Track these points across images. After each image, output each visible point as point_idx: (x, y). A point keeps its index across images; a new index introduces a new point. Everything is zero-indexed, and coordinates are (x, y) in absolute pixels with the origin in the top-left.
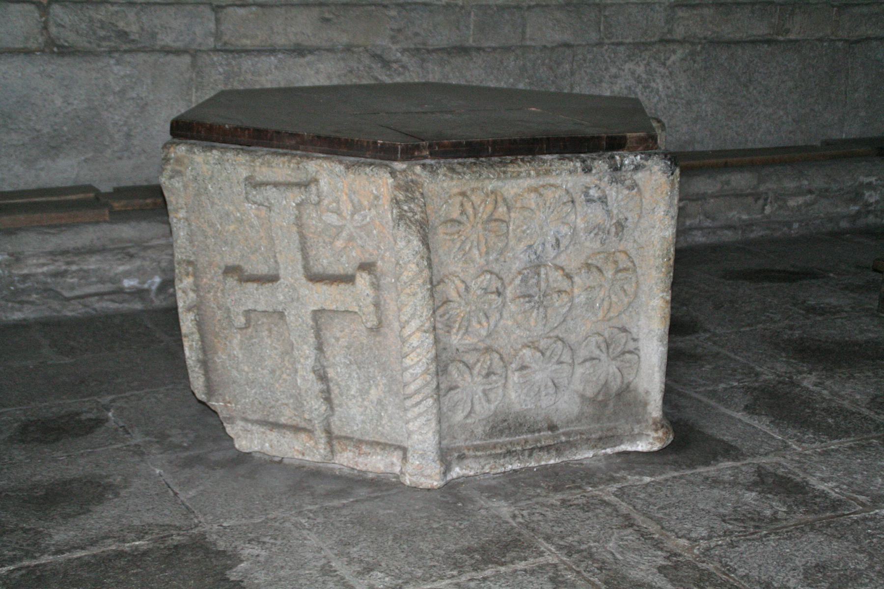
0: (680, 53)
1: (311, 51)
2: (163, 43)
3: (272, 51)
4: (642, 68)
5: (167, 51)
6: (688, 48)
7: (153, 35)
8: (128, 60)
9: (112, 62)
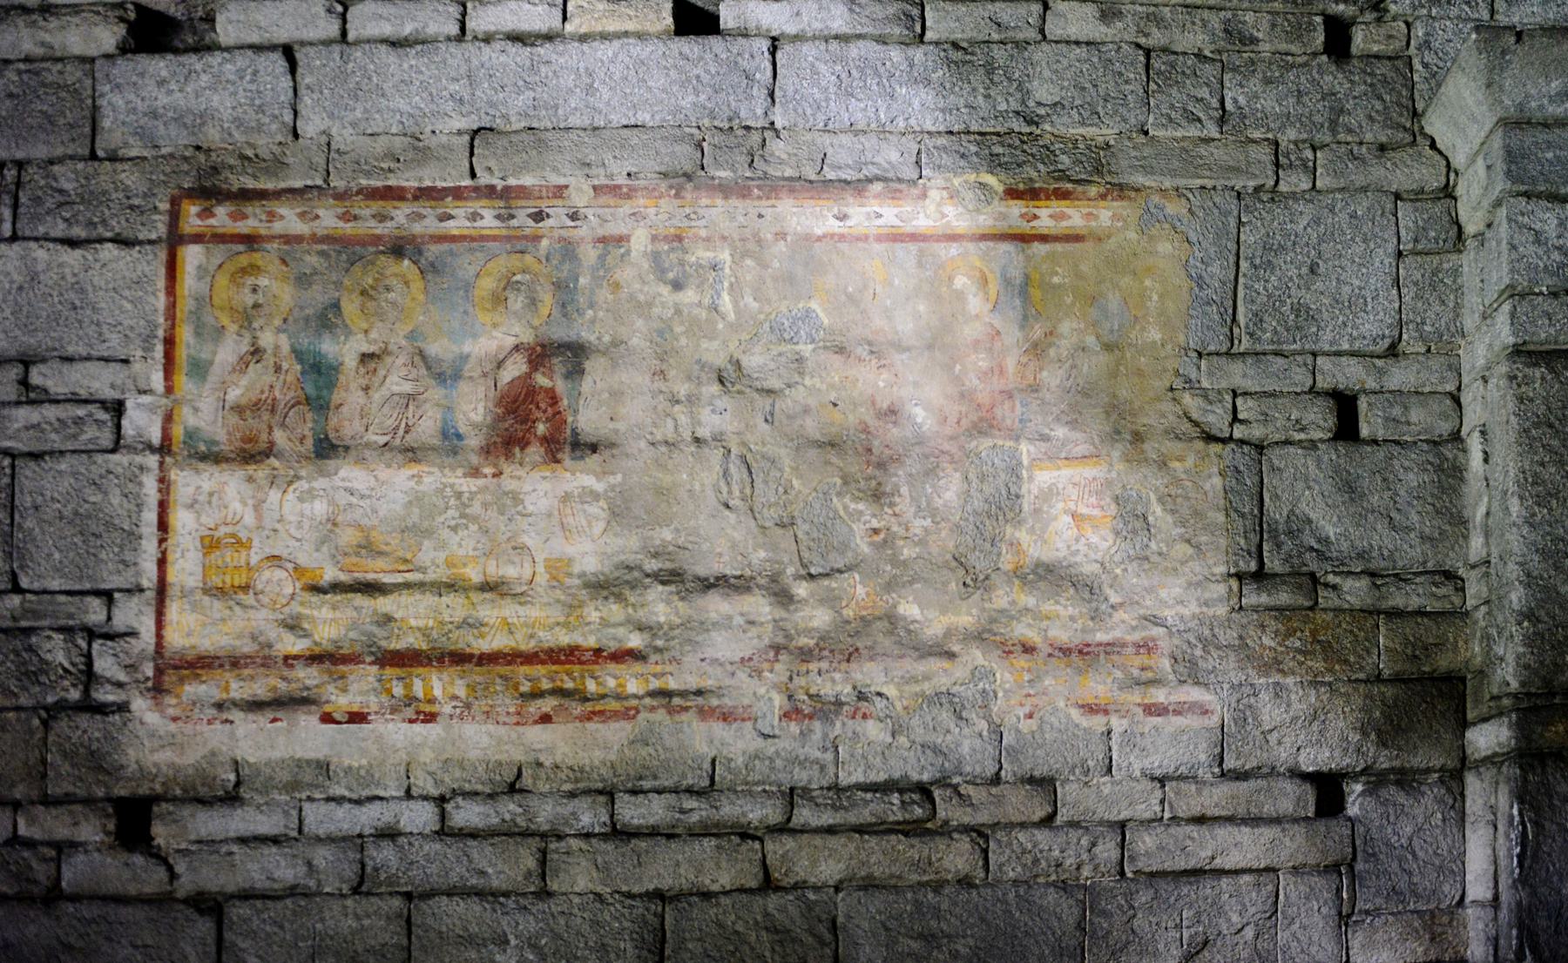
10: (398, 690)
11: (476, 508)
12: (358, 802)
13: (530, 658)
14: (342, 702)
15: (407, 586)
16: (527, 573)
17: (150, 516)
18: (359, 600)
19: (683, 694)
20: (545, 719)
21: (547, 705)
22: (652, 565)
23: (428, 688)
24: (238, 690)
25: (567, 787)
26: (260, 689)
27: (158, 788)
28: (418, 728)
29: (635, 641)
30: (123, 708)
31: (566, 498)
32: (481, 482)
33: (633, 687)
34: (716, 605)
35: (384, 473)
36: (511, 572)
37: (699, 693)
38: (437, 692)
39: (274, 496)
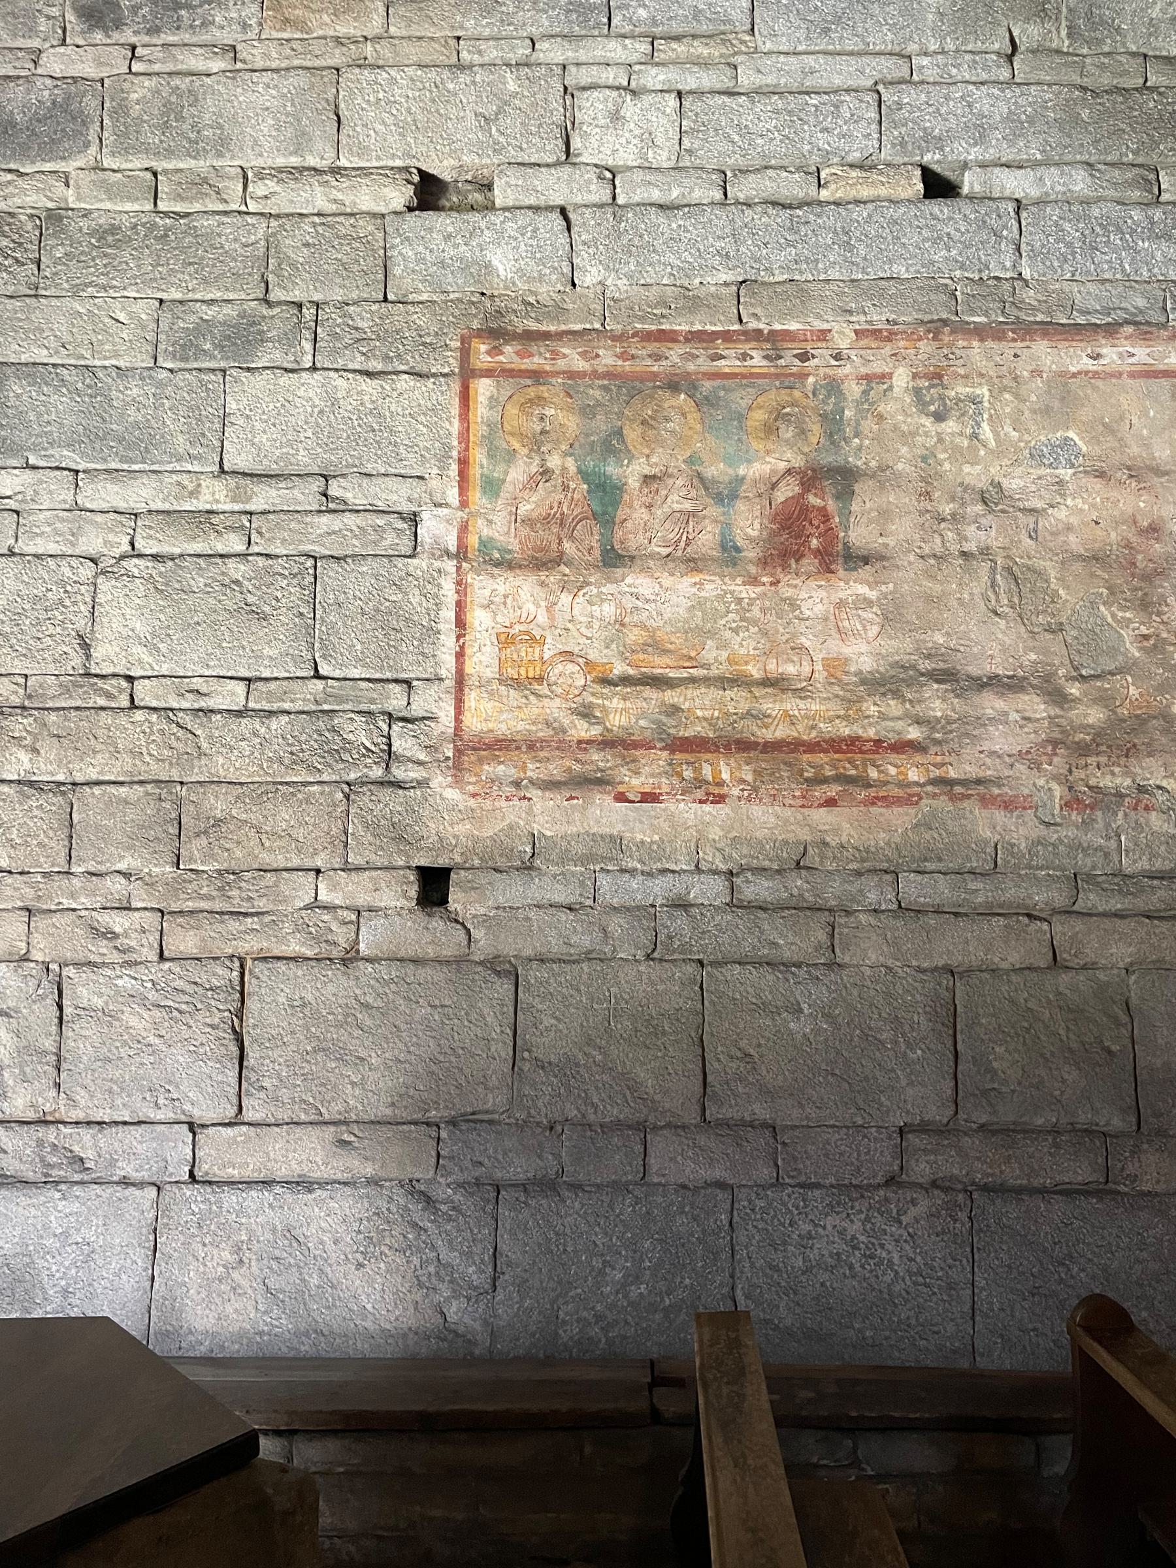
0: (923, 1206)
1: (323, 1184)
2: (123, 1173)
3: (267, 1183)
4: (858, 1225)
5: (125, 1182)
6: (939, 1197)
7: (112, 1163)
8: (78, 1194)
9: (57, 1195)
10: (688, 774)
11: (756, 612)
12: (650, 874)
13: (813, 747)
14: (637, 783)
15: (693, 680)
16: (806, 669)
17: (449, 614)
18: (647, 692)
19: (963, 783)
20: (831, 803)
21: (833, 790)
22: (925, 665)
23: (716, 773)
24: (533, 770)
25: (854, 866)
26: (555, 770)
27: (458, 859)
28: (707, 808)
29: (914, 733)
30: (422, 784)
31: (841, 604)
32: (759, 589)
33: (913, 775)
34: (991, 703)
35: (667, 581)
36: (791, 669)
37: (979, 782)
38: (725, 776)
39: (565, 598)
